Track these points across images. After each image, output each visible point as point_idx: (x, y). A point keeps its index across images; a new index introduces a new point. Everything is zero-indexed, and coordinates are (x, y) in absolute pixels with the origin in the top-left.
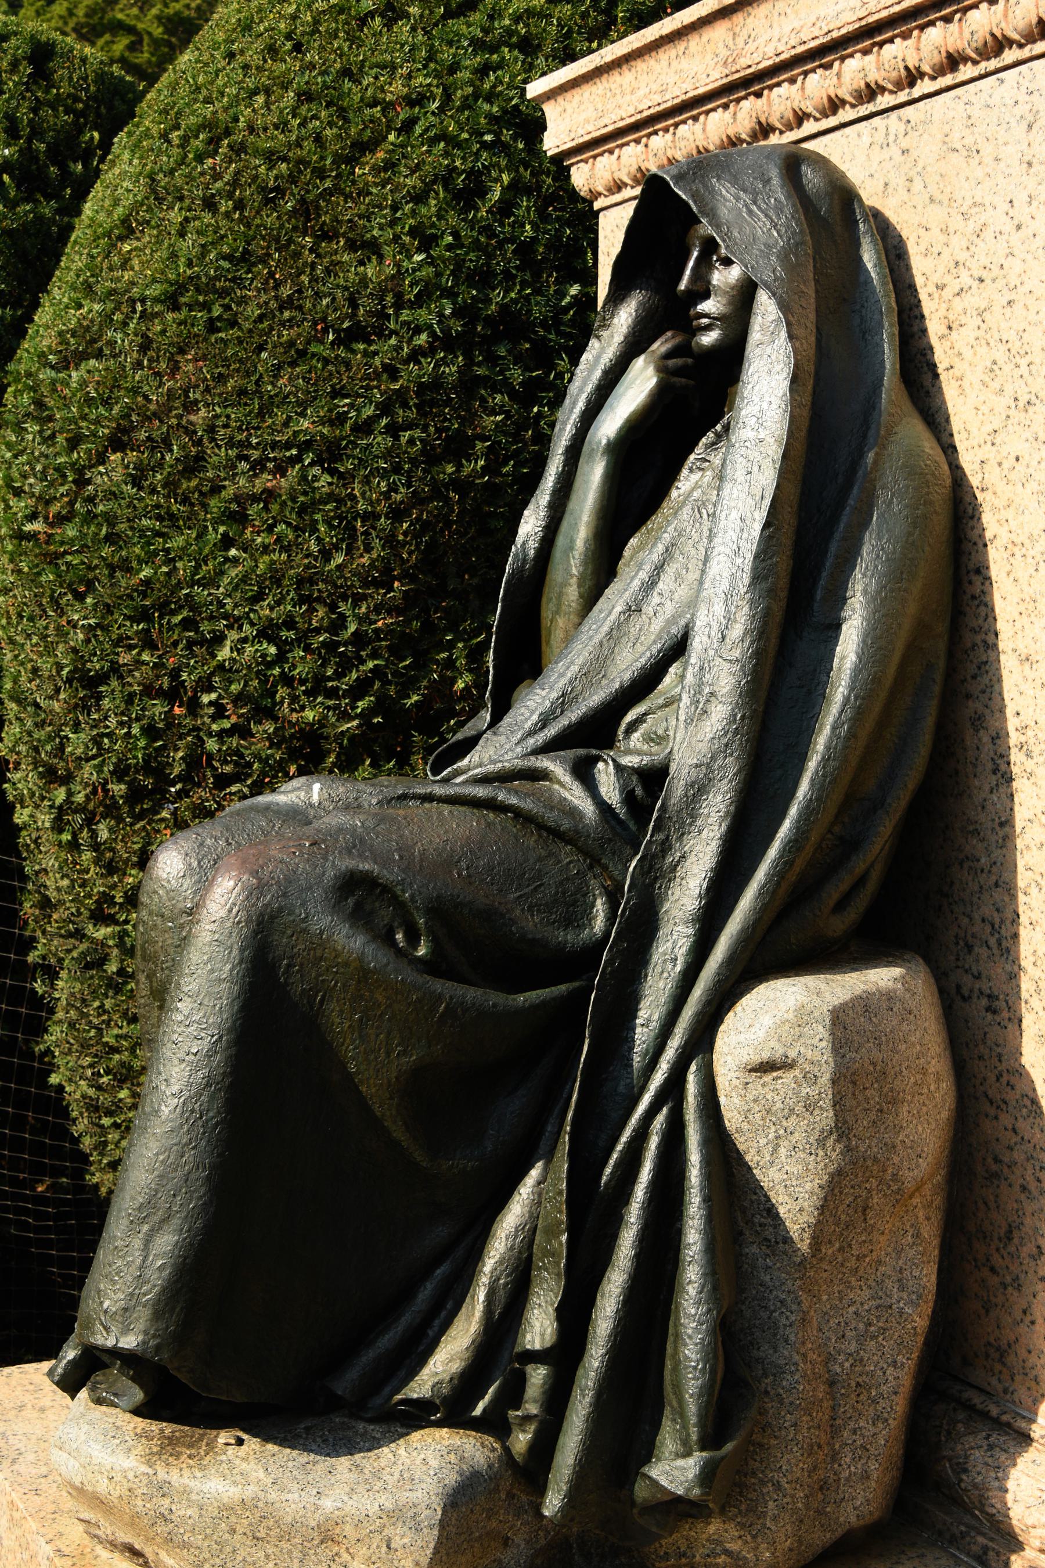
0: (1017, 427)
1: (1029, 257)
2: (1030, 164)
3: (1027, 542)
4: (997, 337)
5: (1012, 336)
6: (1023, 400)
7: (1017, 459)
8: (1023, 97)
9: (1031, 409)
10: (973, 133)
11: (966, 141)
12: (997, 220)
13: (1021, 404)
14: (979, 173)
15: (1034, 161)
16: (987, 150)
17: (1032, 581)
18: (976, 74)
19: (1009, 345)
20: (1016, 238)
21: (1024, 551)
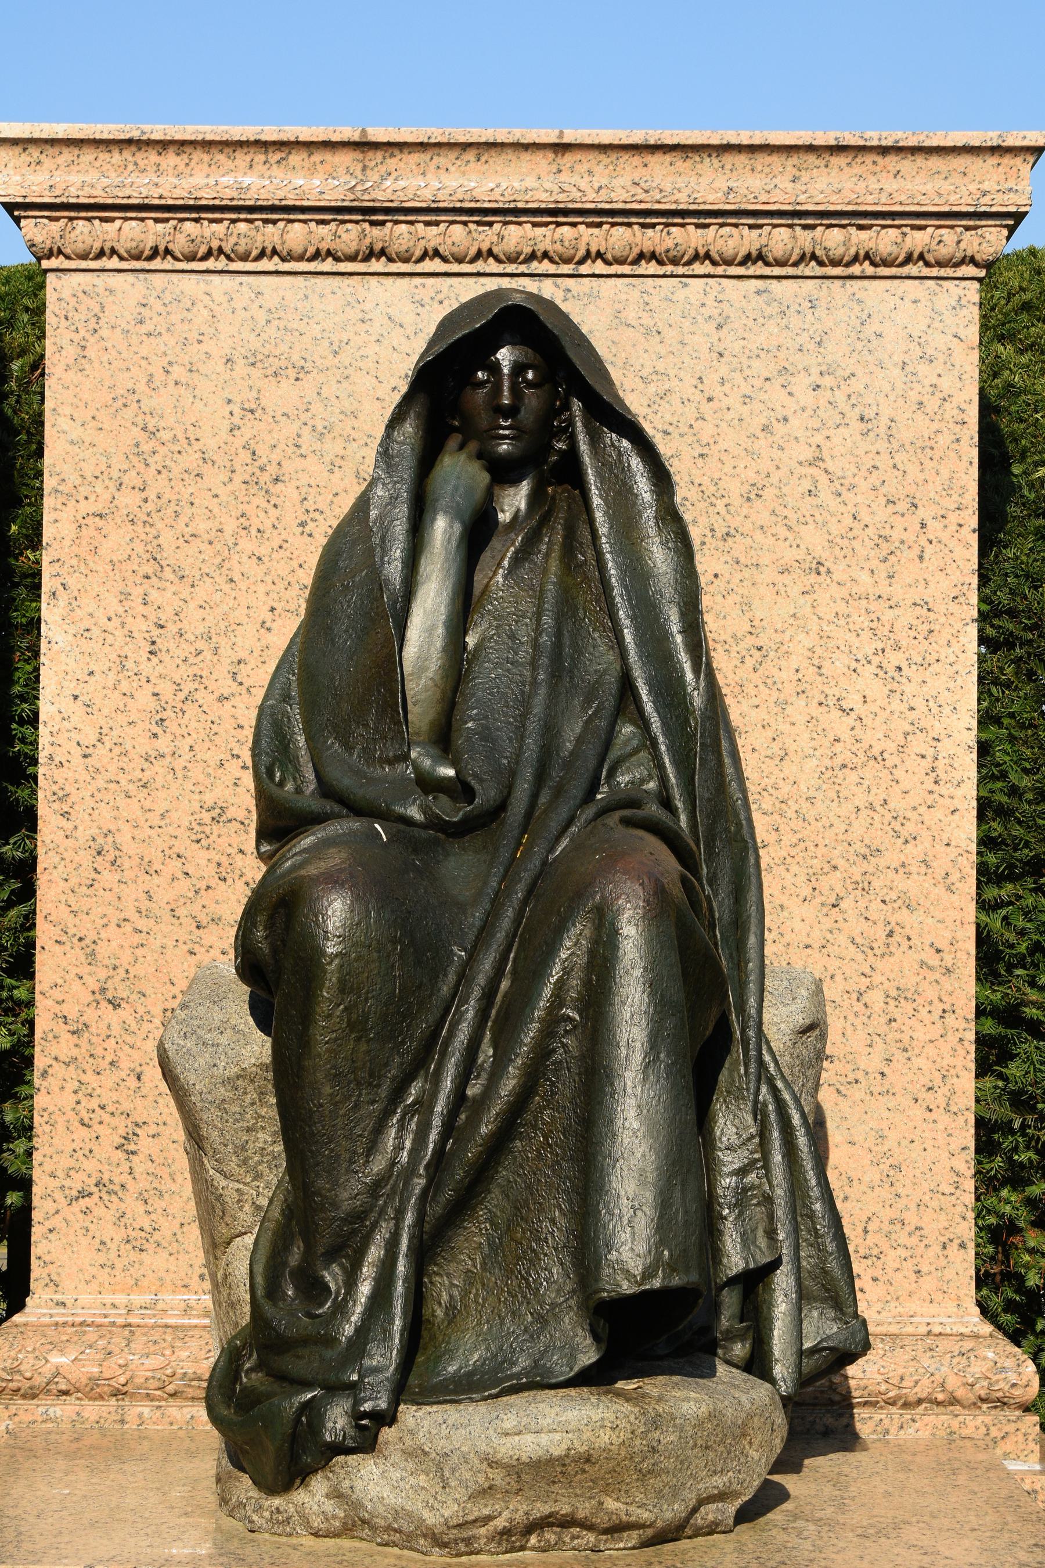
0: (713, 552)
1: (723, 425)
2: (721, 355)
3: (730, 640)
4: (687, 479)
5: (706, 481)
6: (721, 530)
7: (716, 576)
8: (710, 301)
9: (730, 539)
10: (652, 317)
11: (644, 322)
12: (686, 388)
13: (719, 535)
14: (662, 350)
15: (726, 353)
16: (670, 334)
17: (737, 671)
18: (661, 273)
19: (703, 488)
20: (706, 408)
21: (727, 647)
